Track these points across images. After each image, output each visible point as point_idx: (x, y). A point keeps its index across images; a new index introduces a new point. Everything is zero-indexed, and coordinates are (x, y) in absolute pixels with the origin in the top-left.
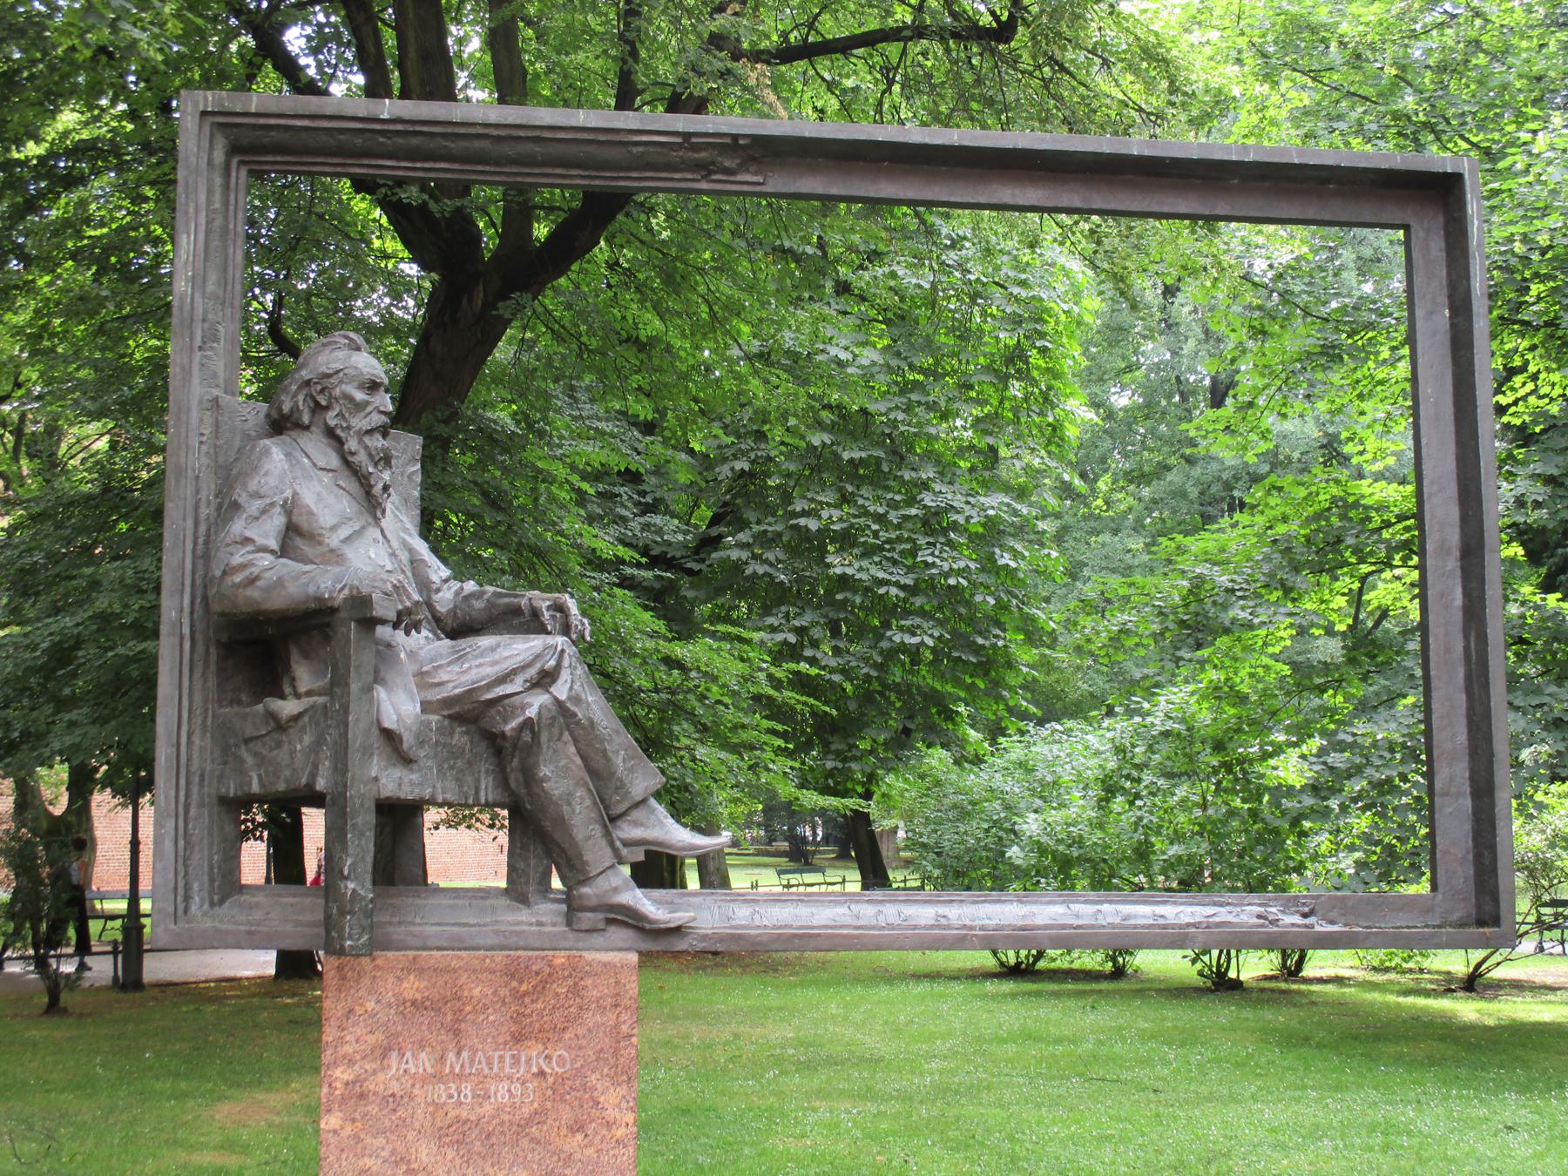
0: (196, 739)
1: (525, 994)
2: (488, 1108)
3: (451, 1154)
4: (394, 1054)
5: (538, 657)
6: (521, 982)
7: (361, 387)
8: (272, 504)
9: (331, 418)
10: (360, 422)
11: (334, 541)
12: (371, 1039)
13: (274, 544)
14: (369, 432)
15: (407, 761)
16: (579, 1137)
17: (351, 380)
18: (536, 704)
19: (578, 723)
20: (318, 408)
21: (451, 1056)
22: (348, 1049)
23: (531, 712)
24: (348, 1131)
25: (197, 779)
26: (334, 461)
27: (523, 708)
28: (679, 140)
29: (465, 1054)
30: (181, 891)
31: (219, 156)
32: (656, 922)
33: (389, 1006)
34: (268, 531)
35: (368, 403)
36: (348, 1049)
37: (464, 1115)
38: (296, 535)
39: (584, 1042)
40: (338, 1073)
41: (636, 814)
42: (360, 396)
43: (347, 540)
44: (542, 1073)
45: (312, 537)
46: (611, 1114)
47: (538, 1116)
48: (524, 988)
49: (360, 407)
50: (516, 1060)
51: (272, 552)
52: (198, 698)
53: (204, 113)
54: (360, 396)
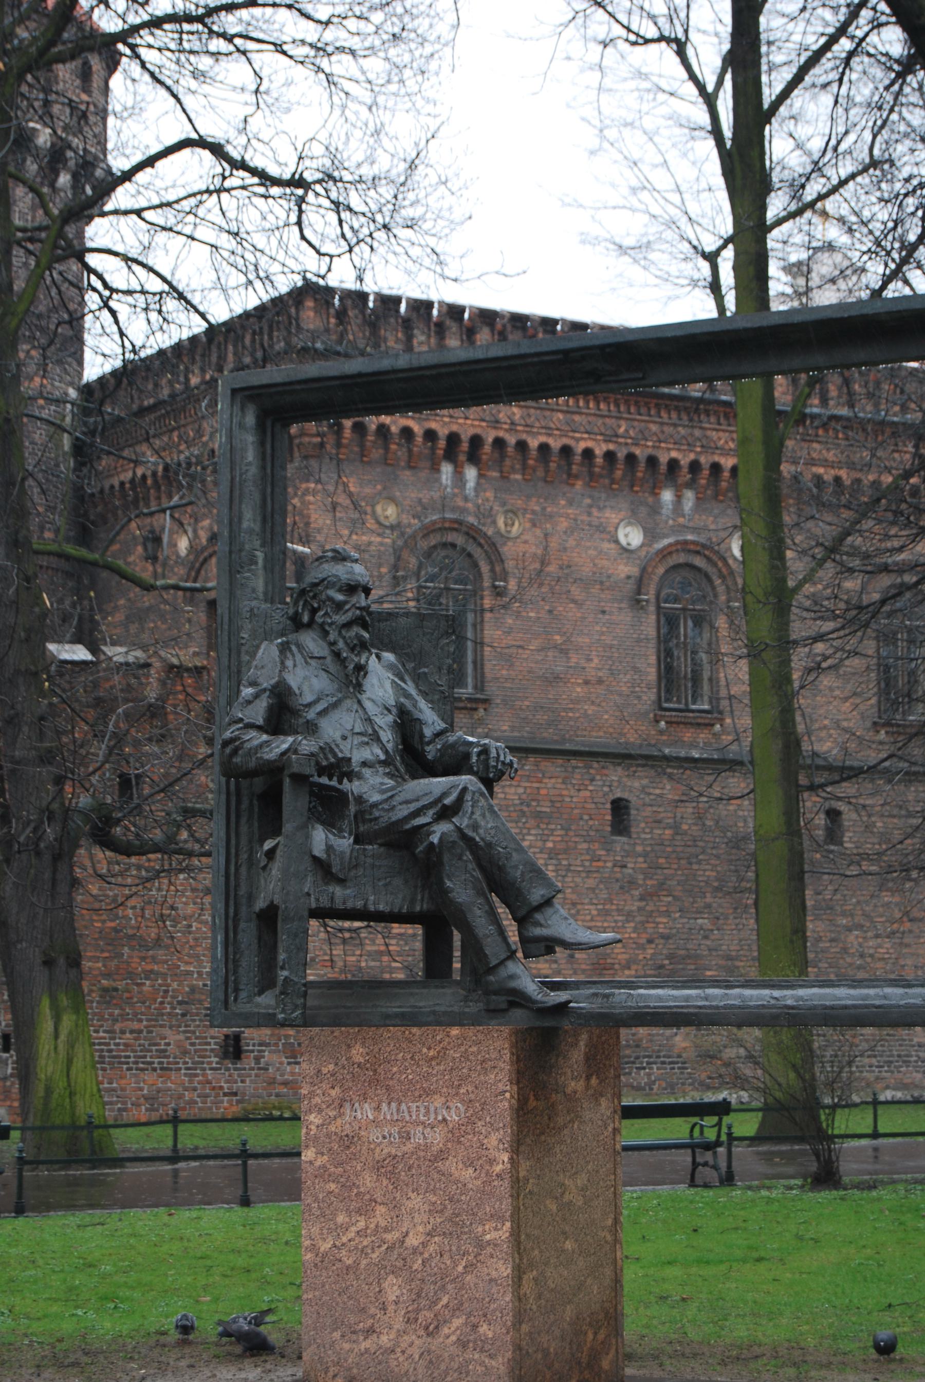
0: (243, 870)
1: (433, 1058)
2: (409, 1147)
3: (385, 1182)
4: (347, 1105)
5: (445, 795)
6: (429, 1049)
7: (340, 590)
8: (265, 690)
9: (319, 618)
10: (341, 619)
11: (311, 715)
12: (333, 1093)
13: (260, 722)
14: (348, 625)
15: (341, 881)
16: (471, 1170)
17: (331, 585)
18: (440, 830)
19: (476, 843)
20: (314, 611)
21: (384, 1106)
22: (317, 1100)
23: (435, 839)
24: (318, 1163)
25: (244, 901)
26: (324, 651)
27: (429, 834)
28: (560, 356)
29: (394, 1105)
30: (231, 985)
31: (250, 419)
32: (536, 1002)
33: (344, 1067)
34: (258, 712)
35: (346, 602)
36: (317, 1100)
37: (393, 1151)
38: (283, 713)
39: (472, 1096)
40: (312, 1117)
41: (538, 916)
42: (340, 597)
43: (323, 713)
44: (444, 1120)
45: (295, 713)
46: (493, 1153)
47: (442, 1155)
48: (431, 1053)
49: (339, 606)
50: (427, 1113)
51: (259, 728)
52: (244, 840)
53: (234, 391)
54: (340, 597)
